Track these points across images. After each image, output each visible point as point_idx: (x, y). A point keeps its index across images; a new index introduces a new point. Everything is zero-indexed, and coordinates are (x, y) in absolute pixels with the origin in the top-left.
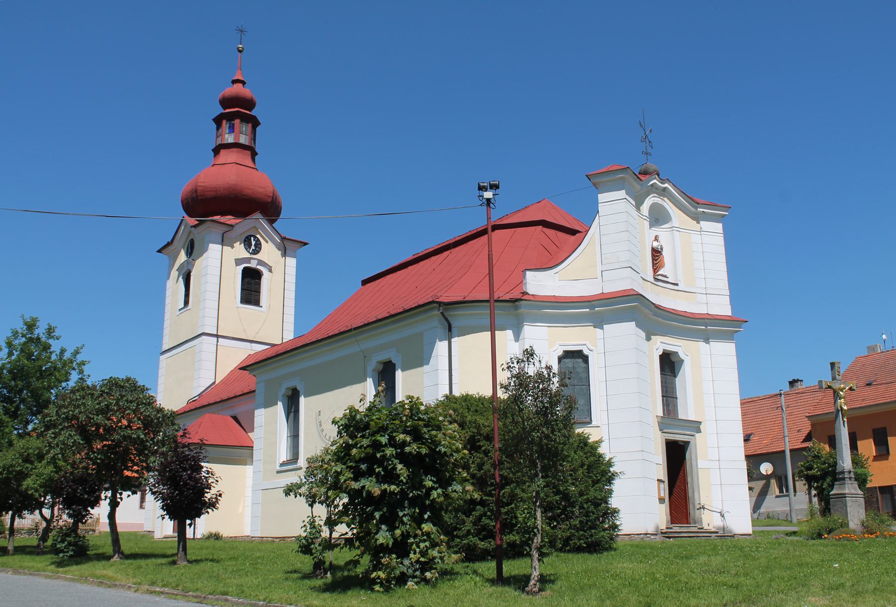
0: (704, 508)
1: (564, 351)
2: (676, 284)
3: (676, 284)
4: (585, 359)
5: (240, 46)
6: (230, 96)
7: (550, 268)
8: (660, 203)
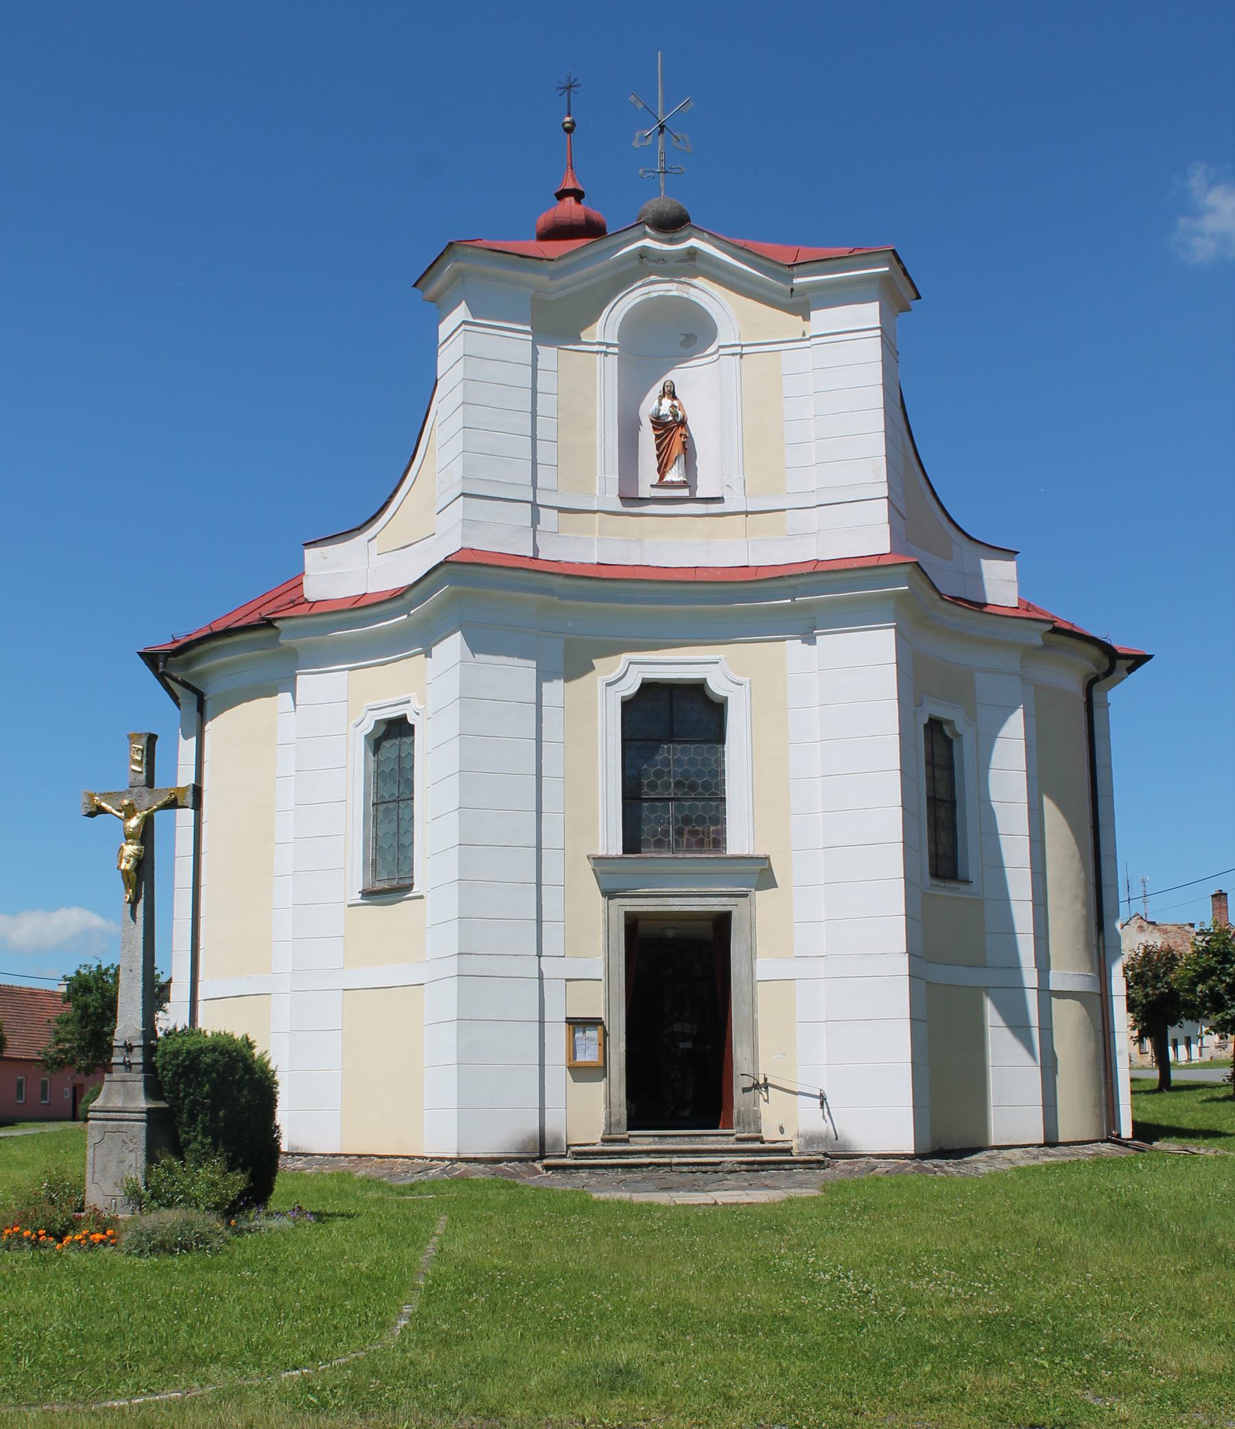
0: (766, 1086)
2: (719, 500)
3: (719, 500)
5: (568, 119)
6: (544, 229)
7: (359, 529)
8: (675, 293)
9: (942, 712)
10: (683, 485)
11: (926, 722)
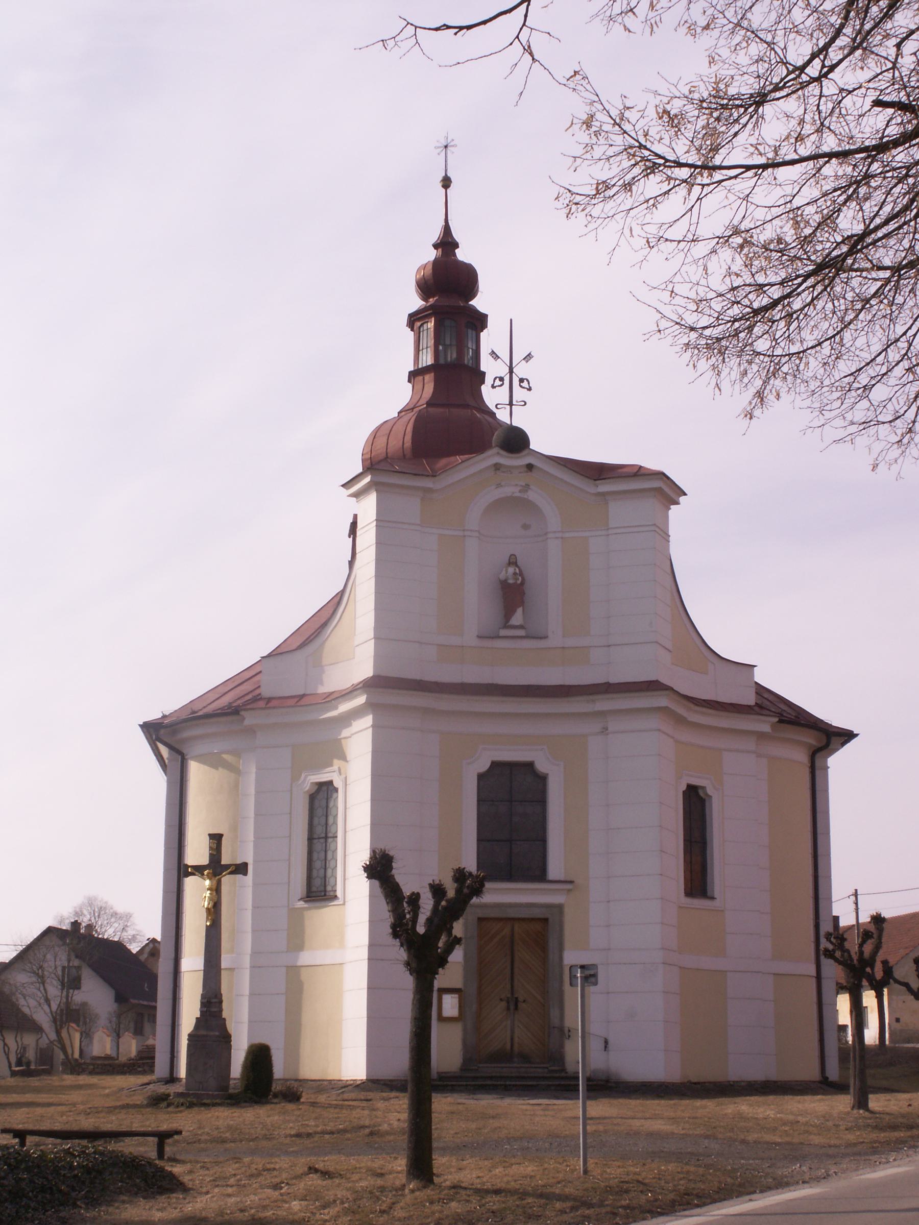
4: (336, 790)
9: (695, 782)
10: (521, 627)
11: (684, 788)
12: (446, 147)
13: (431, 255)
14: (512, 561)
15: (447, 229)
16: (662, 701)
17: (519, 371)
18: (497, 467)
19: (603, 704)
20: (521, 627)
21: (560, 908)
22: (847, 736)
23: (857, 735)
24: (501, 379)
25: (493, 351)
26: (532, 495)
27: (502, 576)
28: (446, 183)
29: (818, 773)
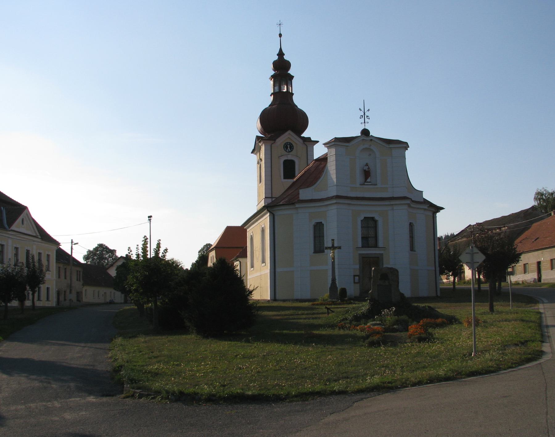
1: (315, 223)
10: (370, 182)
12: (280, 24)
13: (276, 58)
14: (367, 165)
15: (281, 50)
16: (408, 202)
17: (367, 114)
18: (363, 139)
19: (393, 202)
20: (370, 182)
21: (382, 254)
22: (442, 208)
23: (444, 209)
24: (362, 116)
25: (360, 109)
26: (372, 147)
27: (365, 169)
28: (280, 35)
29: (435, 218)
